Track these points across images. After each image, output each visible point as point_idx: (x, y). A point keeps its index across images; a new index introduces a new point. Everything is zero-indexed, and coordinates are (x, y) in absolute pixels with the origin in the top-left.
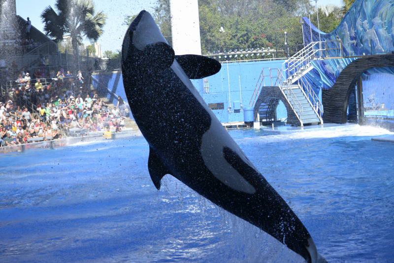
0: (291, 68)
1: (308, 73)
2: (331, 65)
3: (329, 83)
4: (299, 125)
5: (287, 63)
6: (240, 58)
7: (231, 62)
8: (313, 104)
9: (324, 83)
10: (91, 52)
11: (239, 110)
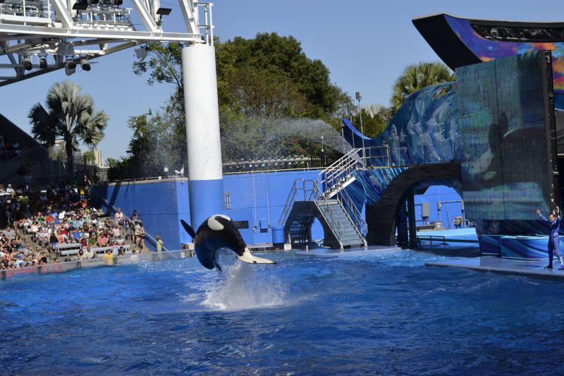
0: (329, 180)
1: (348, 186)
2: (376, 177)
4: (339, 247)
5: (324, 174)
8: (355, 223)
10: (89, 160)
11: (266, 229)
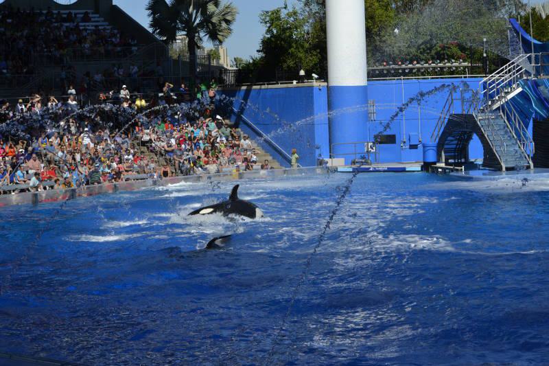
0: (492, 89)
1: (513, 97)
3: (543, 113)
4: (500, 169)
5: (485, 83)
6: (420, 74)
7: (408, 79)
8: (520, 141)
9: (536, 111)
